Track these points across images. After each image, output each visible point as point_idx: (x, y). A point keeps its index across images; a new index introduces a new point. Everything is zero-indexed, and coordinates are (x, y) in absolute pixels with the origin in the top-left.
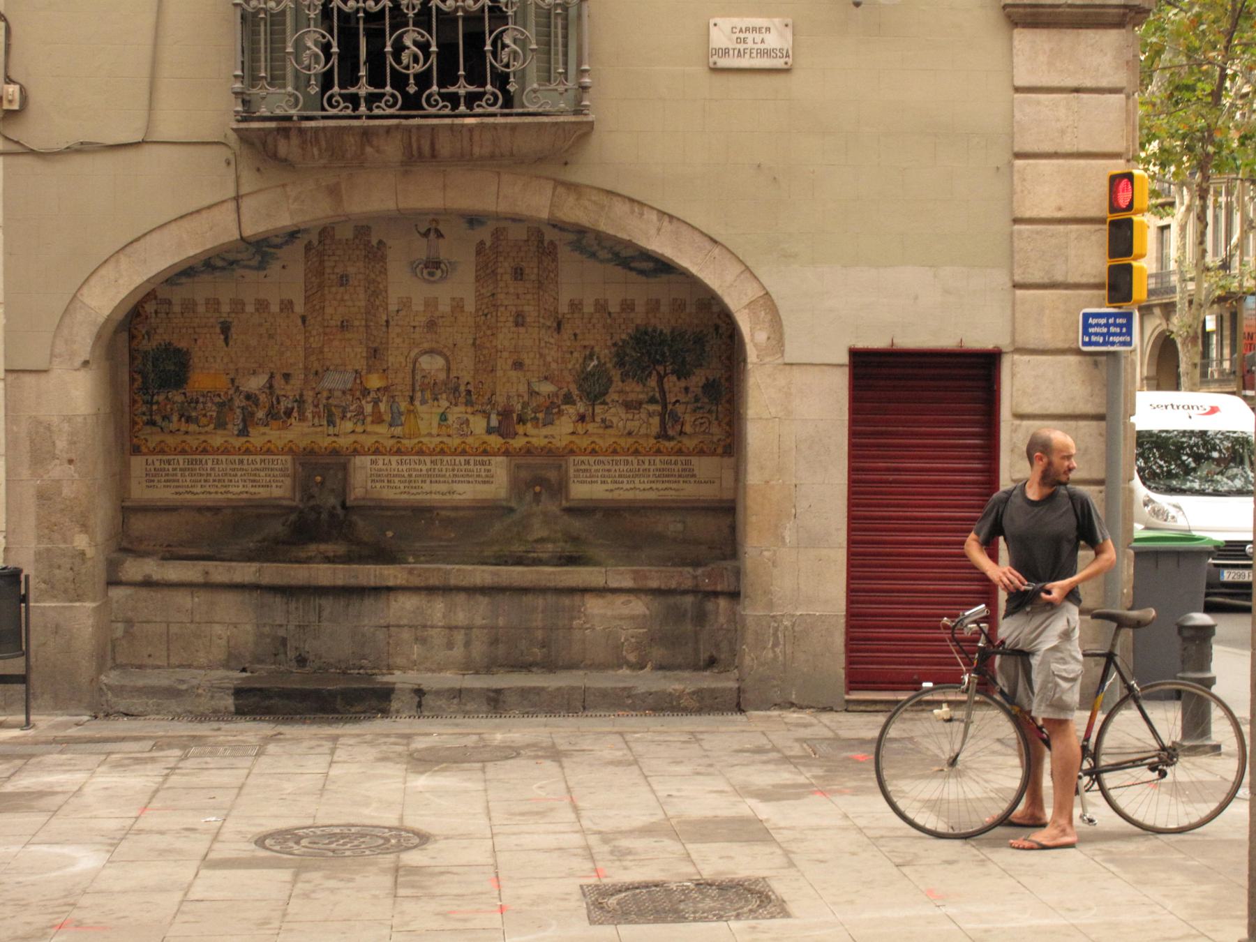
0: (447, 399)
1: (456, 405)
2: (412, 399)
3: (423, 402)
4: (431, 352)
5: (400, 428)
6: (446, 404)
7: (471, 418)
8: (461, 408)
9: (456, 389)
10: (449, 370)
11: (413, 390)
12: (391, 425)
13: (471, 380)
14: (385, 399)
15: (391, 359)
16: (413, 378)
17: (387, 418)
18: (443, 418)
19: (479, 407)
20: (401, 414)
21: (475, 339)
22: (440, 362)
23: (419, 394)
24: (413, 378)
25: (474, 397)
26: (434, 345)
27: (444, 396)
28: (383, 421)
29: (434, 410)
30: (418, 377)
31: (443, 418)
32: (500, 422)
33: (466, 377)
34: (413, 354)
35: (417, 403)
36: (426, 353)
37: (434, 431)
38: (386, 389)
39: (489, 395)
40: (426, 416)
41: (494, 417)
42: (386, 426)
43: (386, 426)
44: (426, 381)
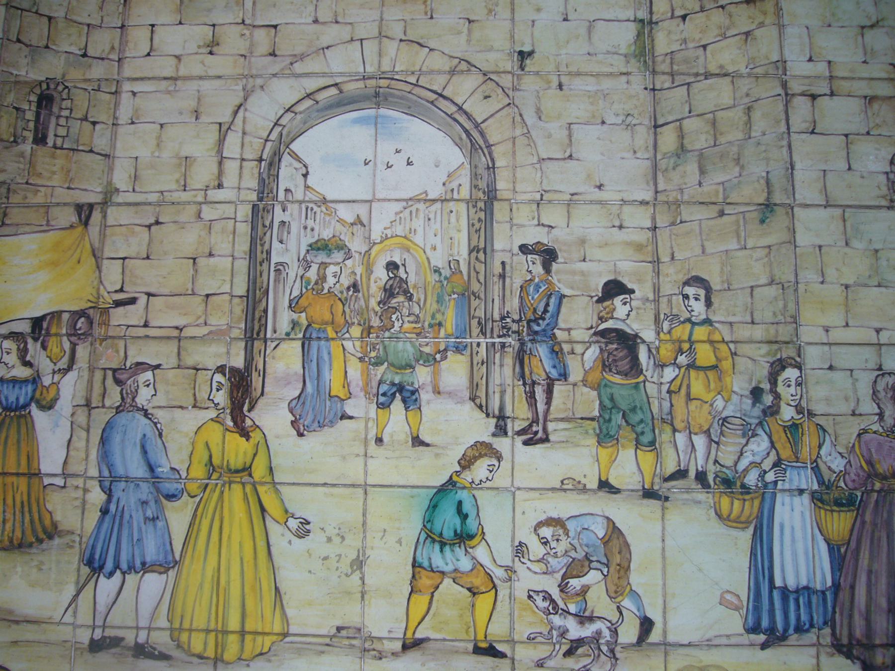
0: (476, 397)
1: (534, 437)
2: (242, 388)
3: (313, 413)
4: (377, 95)
5: (153, 583)
6: (480, 429)
7: (636, 520)
8: (572, 457)
9: (536, 325)
10: (486, 201)
11: (255, 332)
12: (95, 565)
13: (628, 269)
14: (70, 388)
15: (133, 144)
16: (257, 254)
17: (75, 511)
18: (449, 520)
19: (681, 450)
20: (163, 490)
21: (646, 26)
22: (429, 155)
23: (284, 361)
24: (257, 254)
25: (657, 381)
26: (399, 59)
27: (455, 372)
28: (52, 532)
29: (384, 467)
30: (287, 252)
31: (449, 520)
32: (840, 556)
33: (599, 248)
34: (263, 112)
35: (272, 417)
36: (344, 103)
37: (385, 619)
38: (85, 323)
39: (752, 368)
40: (323, 508)
41: (793, 515)
42: (62, 563)
43: (62, 563)
44: (338, 275)
